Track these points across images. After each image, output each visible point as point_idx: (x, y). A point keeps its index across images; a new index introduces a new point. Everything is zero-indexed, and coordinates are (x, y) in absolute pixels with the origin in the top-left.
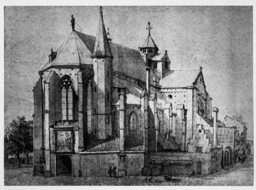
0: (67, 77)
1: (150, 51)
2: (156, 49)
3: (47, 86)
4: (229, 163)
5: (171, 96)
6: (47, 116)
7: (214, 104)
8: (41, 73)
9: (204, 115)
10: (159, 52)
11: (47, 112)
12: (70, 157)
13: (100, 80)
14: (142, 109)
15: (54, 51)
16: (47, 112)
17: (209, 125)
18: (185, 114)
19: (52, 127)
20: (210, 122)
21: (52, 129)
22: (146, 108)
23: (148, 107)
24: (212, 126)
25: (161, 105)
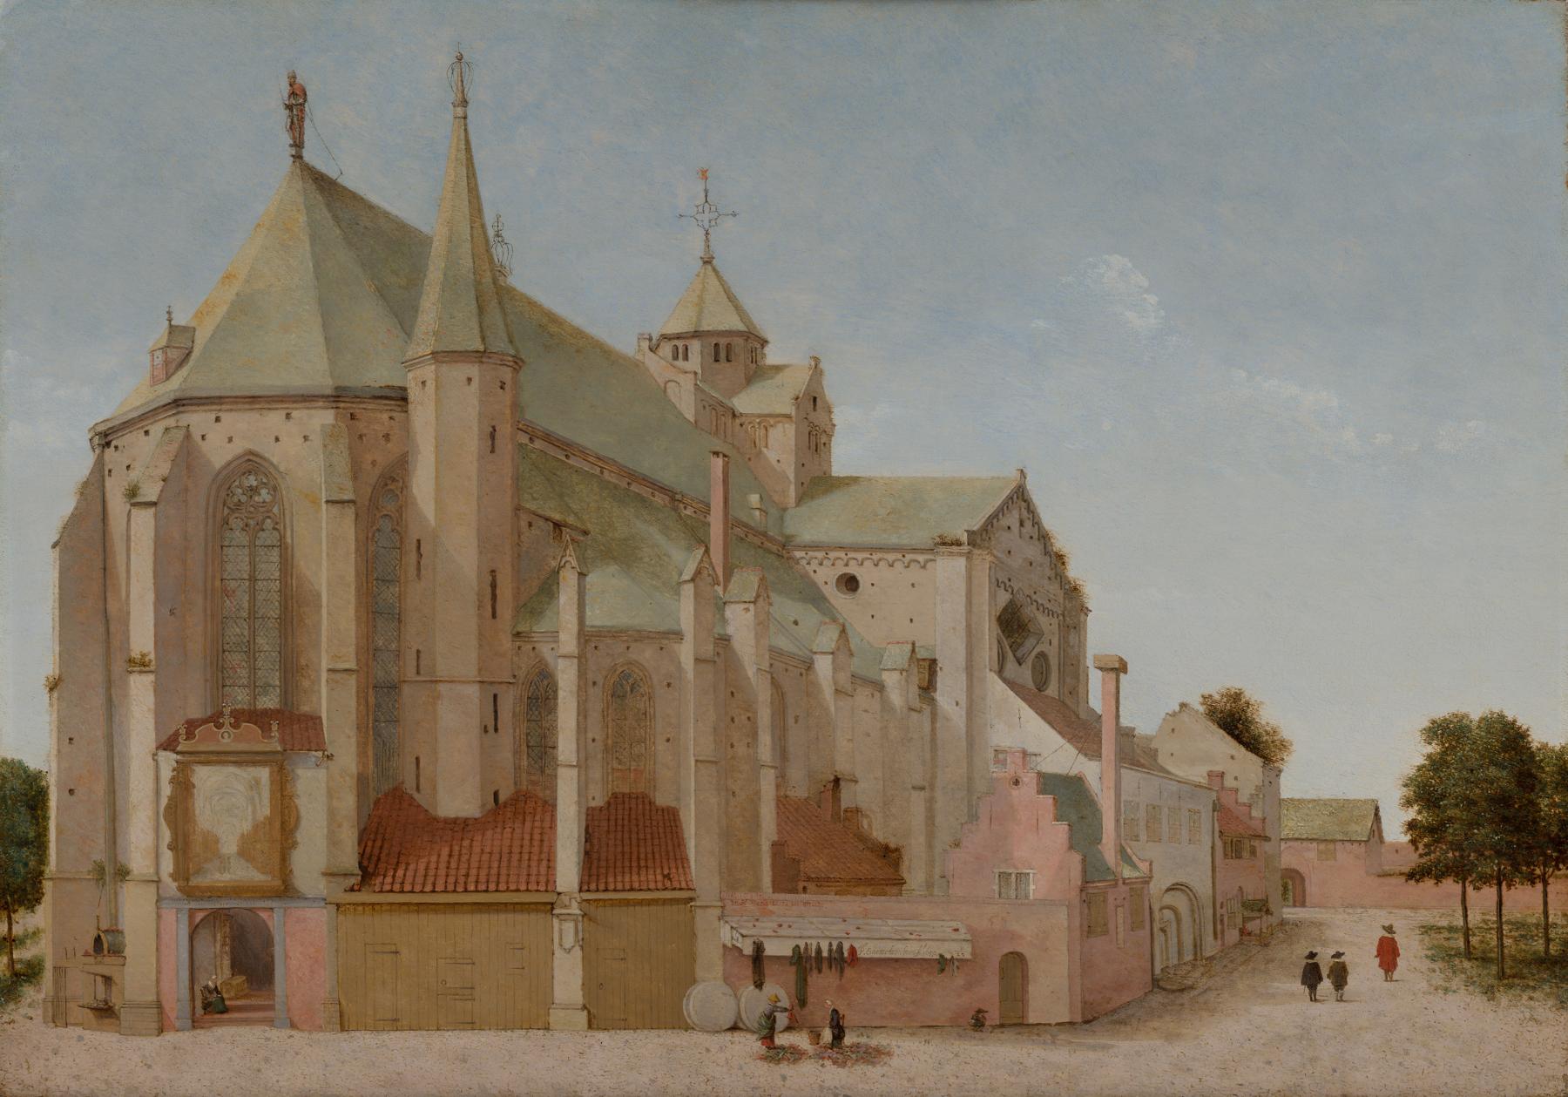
0: (252, 462)
1: (723, 355)
2: (754, 341)
3: (144, 521)
4: (1189, 957)
5: (850, 583)
6: (141, 690)
7: (1101, 635)
8: (105, 438)
9: (1052, 690)
10: (772, 356)
11: (141, 665)
12: (264, 915)
13: (448, 489)
14: (686, 653)
15: (180, 320)
16: (141, 665)
17: (1070, 750)
18: (928, 689)
19: (168, 744)
20: (1080, 729)
21: (168, 760)
22: (708, 649)
23: (724, 640)
24: (1095, 754)
25: (840, 600)
